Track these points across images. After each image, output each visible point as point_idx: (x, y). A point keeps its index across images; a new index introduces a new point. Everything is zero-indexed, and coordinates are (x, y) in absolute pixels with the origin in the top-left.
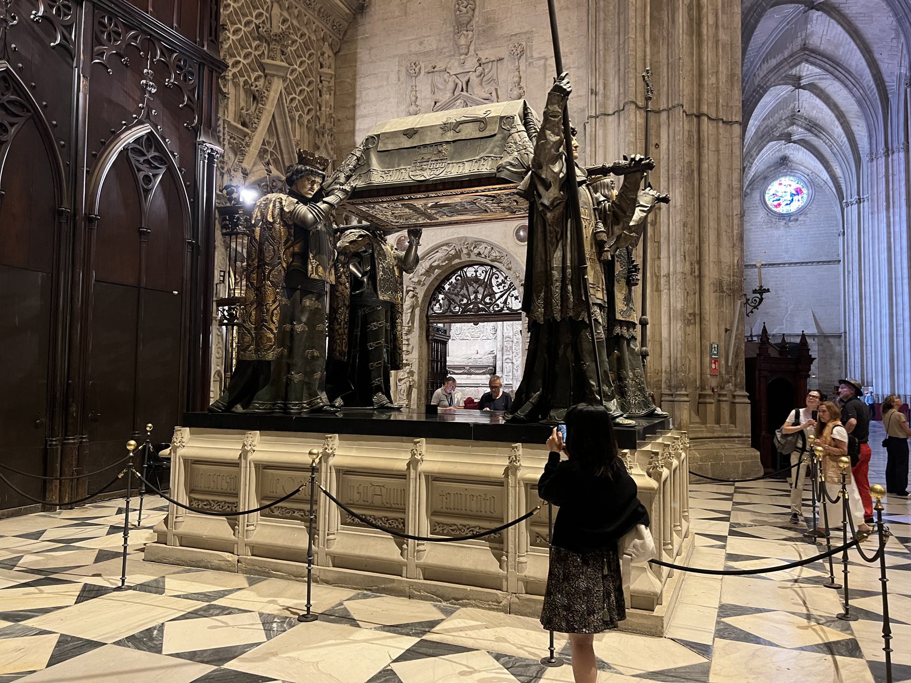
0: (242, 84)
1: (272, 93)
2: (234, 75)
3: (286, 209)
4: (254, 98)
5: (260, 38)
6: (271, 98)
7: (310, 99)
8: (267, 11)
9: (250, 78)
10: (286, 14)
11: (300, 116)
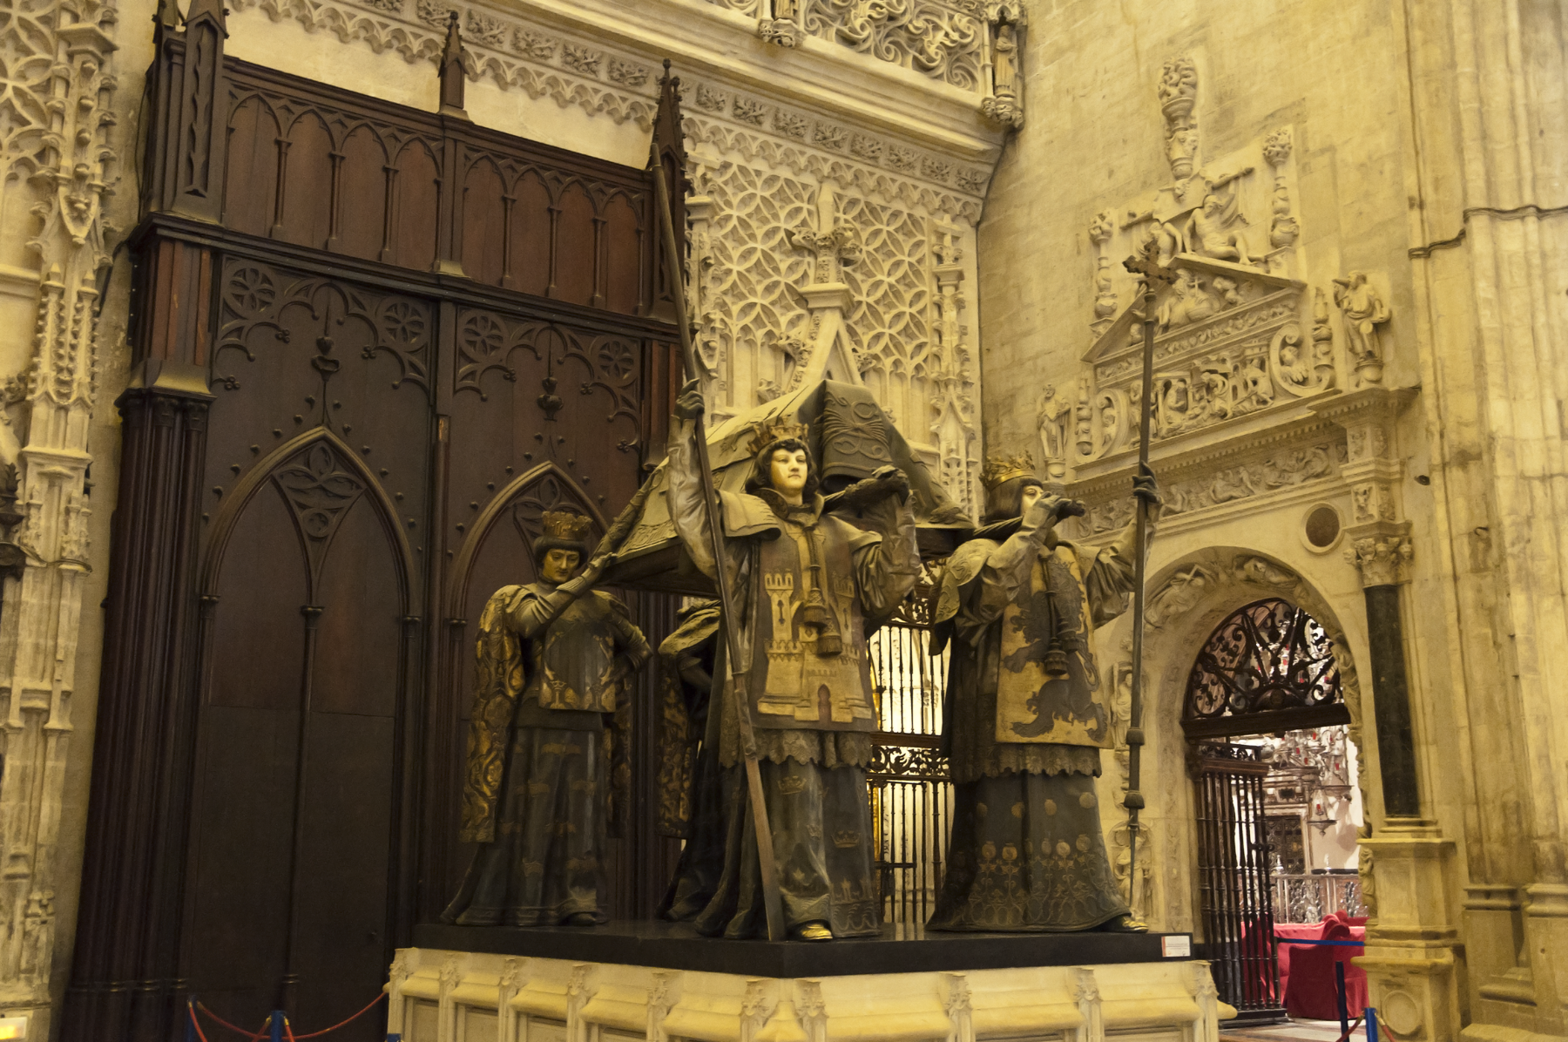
4: (788, 357)
5: (797, 249)
7: (919, 325)
11: (896, 363)
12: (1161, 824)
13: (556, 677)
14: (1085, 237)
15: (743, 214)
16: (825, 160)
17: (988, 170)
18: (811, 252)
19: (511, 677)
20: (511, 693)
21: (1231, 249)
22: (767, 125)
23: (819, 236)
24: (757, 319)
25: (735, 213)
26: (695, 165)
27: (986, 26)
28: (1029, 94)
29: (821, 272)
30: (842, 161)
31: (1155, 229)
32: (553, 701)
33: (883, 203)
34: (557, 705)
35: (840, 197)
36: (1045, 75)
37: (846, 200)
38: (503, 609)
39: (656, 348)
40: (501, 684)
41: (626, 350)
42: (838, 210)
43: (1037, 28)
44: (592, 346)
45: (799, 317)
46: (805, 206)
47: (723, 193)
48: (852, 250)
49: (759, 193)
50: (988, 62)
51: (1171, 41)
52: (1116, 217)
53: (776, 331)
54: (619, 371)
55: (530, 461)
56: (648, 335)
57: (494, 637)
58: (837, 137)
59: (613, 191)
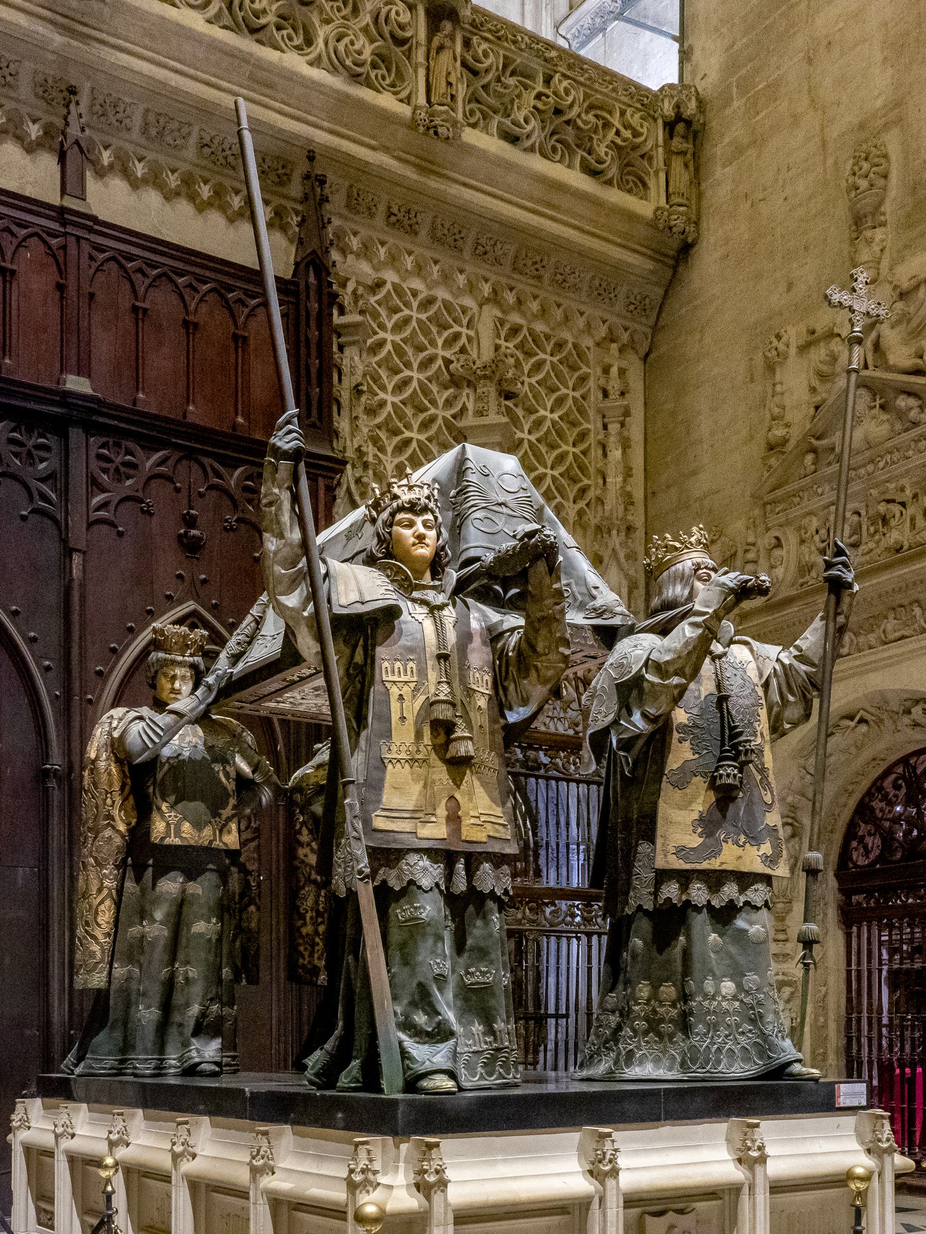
14: (759, 360)
15: (397, 338)
17: (661, 291)
21: (919, 361)
23: (479, 364)
25: (389, 337)
26: (344, 285)
31: (836, 346)
32: (168, 834)
33: (547, 330)
35: (502, 322)
37: (507, 326)
38: (110, 733)
46: (464, 331)
47: (376, 315)
48: (514, 380)
49: (415, 314)
52: (794, 334)
57: (102, 764)
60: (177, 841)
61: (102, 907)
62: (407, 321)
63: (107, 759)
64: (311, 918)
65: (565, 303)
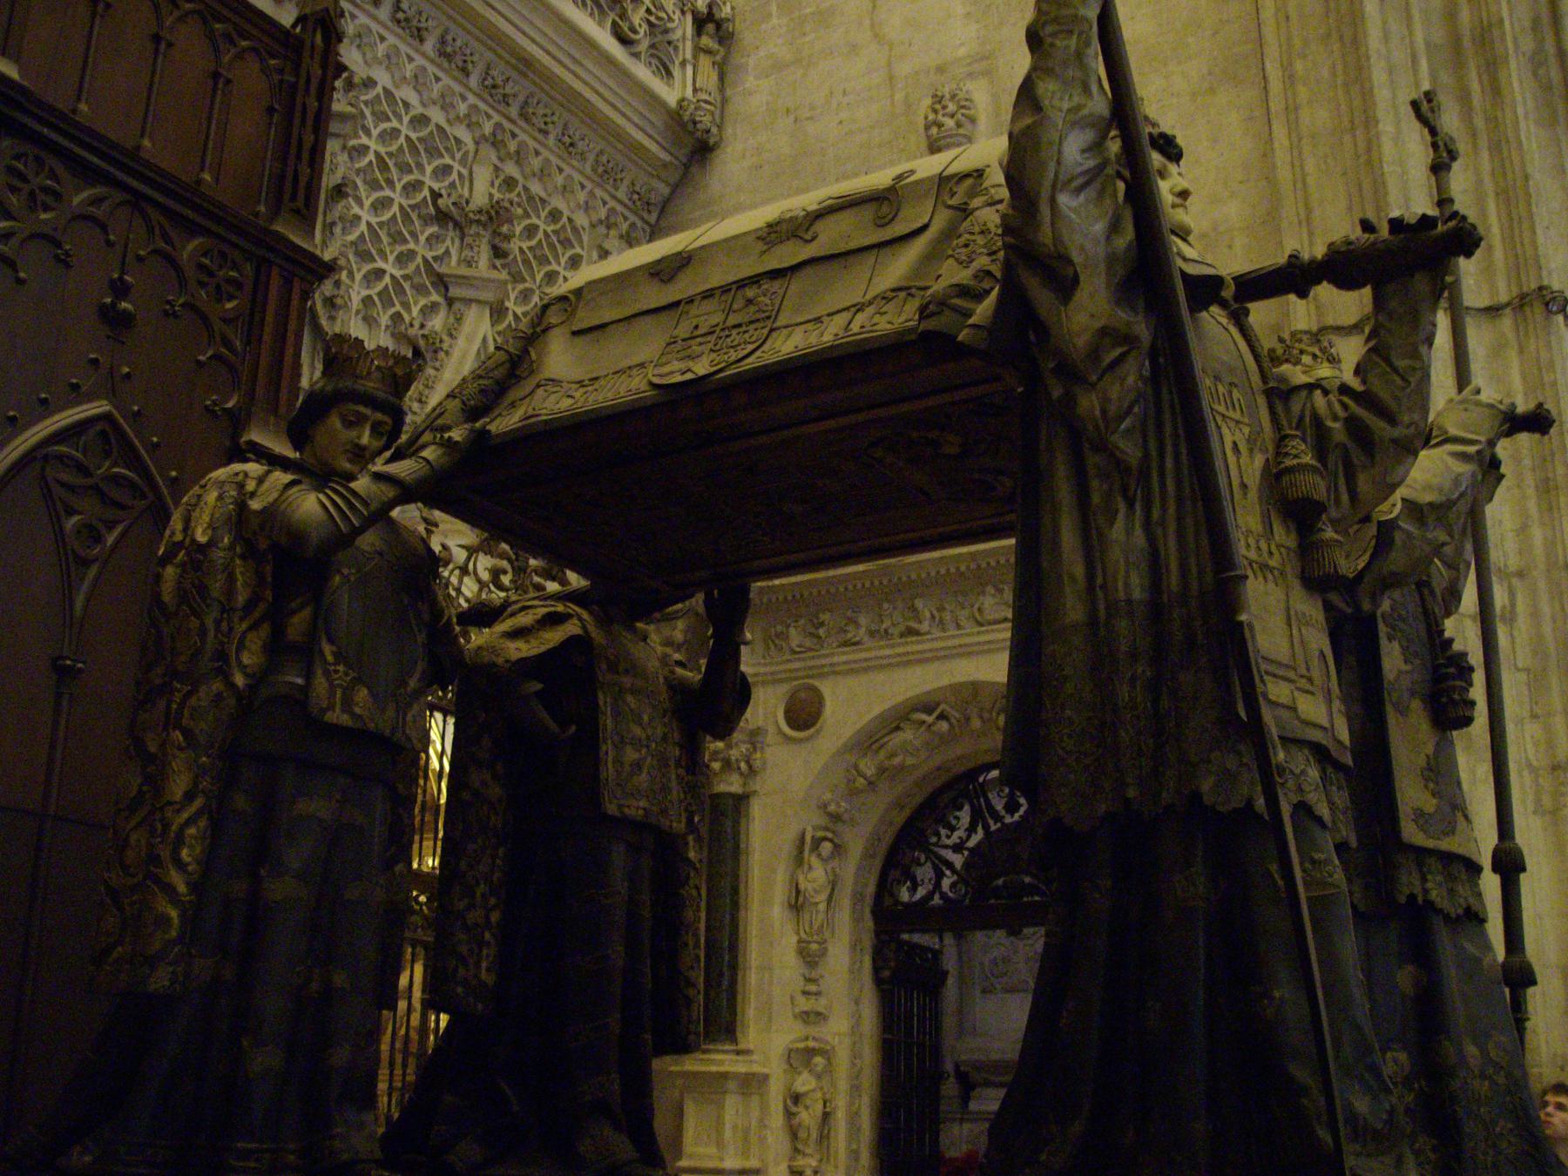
0: (384, 320)
1: (461, 342)
2: (367, 301)
3: (255, 505)
5: (442, 217)
6: (456, 353)
8: (463, 162)
9: (409, 309)
10: (511, 169)
12: (847, 1041)
13: (339, 657)
16: (489, 117)
17: (666, 191)
18: (457, 225)
19: (241, 646)
20: (239, 680)
22: (429, 45)
23: (472, 207)
24: (383, 294)
25: (373, 145)
27: (689, 18)
28: (730, 108)
29: (467, 253)
30: (507, 125)
32: (331, 707)
33: (543, 194)
34: (338, 717)
36: (755, 91)
39: (276, 282)
40: (221, 656)
41: (235, 266)
42: (492, 184)
43: (746, 34)
44: (190, 249)
45: (434, 307)
46: (456, 166)
49: (404, 131)
50: (689, 56)
51: (940, 70)
53: (406, 316)
54: (220, 295)
55: (77, 394)
56: (272, 257)
57: (219, 555)
58: (508, 90)
59: (244, 43)
60: (345, 720)
61: (192, 831)
62: (395, 133)
63: (232, 547)
64: (483, 895)
65: (568, 170)
